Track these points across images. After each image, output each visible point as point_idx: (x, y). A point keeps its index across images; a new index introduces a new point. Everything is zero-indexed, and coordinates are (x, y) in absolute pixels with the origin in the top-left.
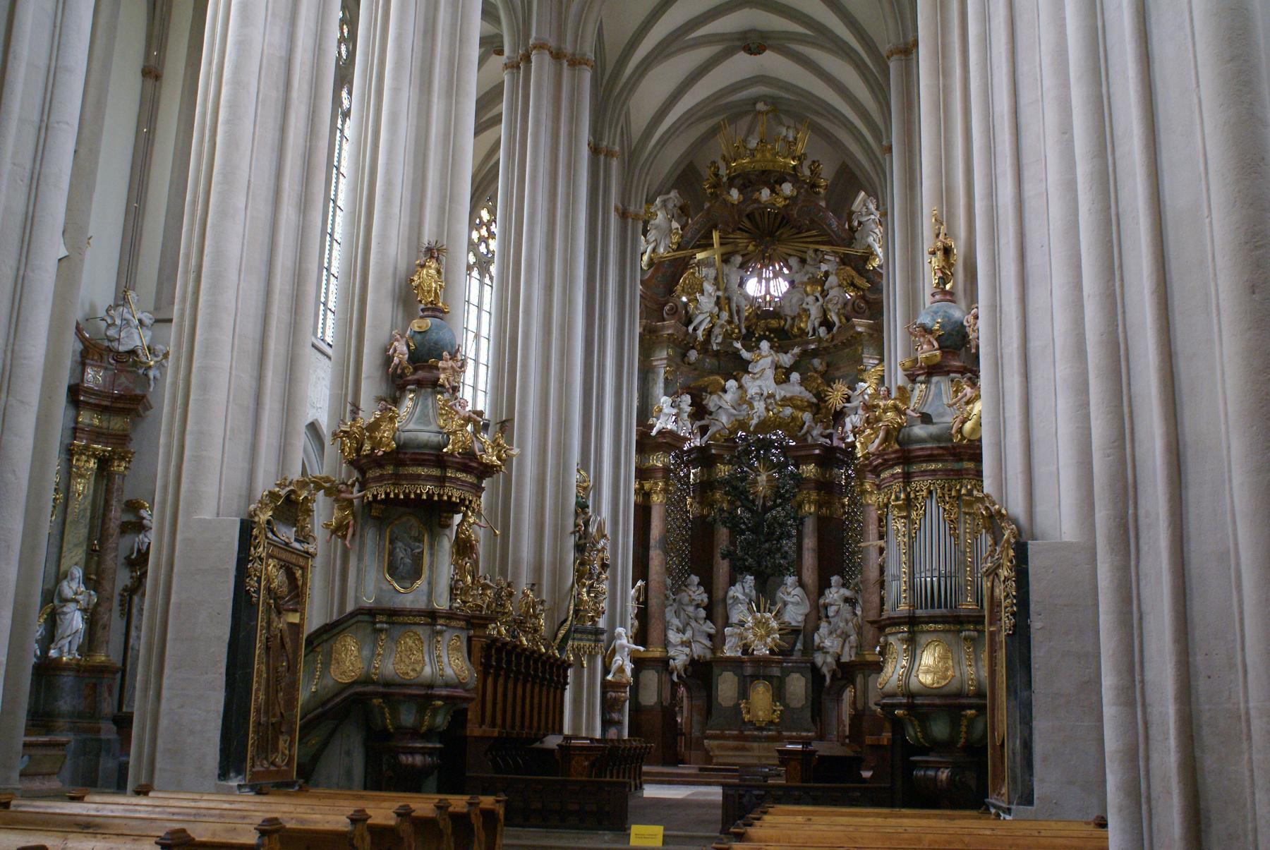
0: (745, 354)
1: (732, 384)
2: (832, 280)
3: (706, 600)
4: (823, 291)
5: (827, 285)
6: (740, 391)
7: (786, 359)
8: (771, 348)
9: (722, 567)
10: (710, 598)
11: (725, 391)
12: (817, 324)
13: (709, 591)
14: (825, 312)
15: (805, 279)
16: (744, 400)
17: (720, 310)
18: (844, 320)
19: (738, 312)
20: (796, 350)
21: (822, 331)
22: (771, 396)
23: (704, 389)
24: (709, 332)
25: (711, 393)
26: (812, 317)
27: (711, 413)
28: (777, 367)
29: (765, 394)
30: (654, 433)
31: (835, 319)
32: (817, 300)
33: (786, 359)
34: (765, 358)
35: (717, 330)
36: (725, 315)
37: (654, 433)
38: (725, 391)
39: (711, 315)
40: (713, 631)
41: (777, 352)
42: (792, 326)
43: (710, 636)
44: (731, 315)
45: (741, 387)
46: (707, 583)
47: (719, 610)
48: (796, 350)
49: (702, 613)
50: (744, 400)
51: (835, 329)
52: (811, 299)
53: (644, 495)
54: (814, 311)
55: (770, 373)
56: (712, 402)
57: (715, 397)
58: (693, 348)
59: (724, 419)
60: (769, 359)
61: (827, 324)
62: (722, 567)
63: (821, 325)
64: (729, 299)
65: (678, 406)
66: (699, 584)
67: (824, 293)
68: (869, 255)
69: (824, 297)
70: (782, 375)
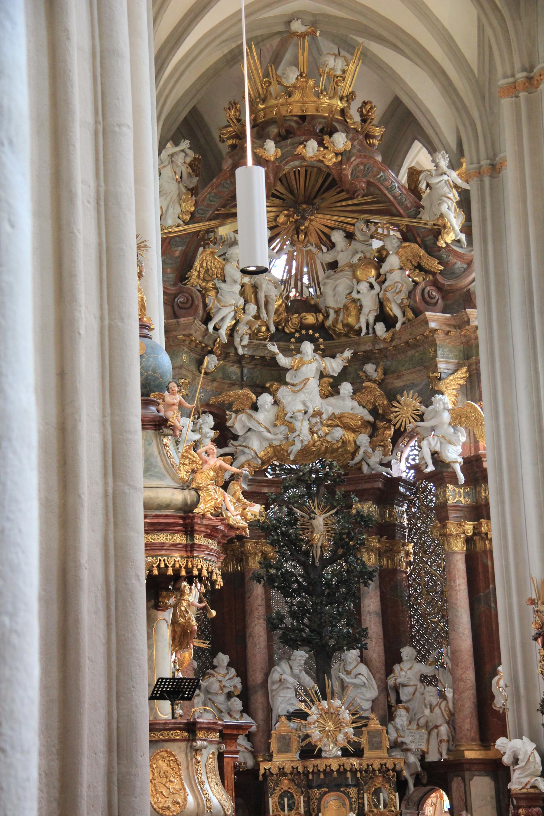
1: (266, 399)
4: (379, 275)
6: (276, 408)
7: (335, 366)
11: (255, 407)
21: (380, 328)
31: (396, 311)
32: (372, 287)
33: (335, 366)
35: (243, 329)
50: (283, 419)
51: (398, 325)
52: (363, 287)
55: (313, 384)
56: (238, 423)
57: (242, 417)
58: (211, 352)
60: (314, 365)
63: (377, 319)
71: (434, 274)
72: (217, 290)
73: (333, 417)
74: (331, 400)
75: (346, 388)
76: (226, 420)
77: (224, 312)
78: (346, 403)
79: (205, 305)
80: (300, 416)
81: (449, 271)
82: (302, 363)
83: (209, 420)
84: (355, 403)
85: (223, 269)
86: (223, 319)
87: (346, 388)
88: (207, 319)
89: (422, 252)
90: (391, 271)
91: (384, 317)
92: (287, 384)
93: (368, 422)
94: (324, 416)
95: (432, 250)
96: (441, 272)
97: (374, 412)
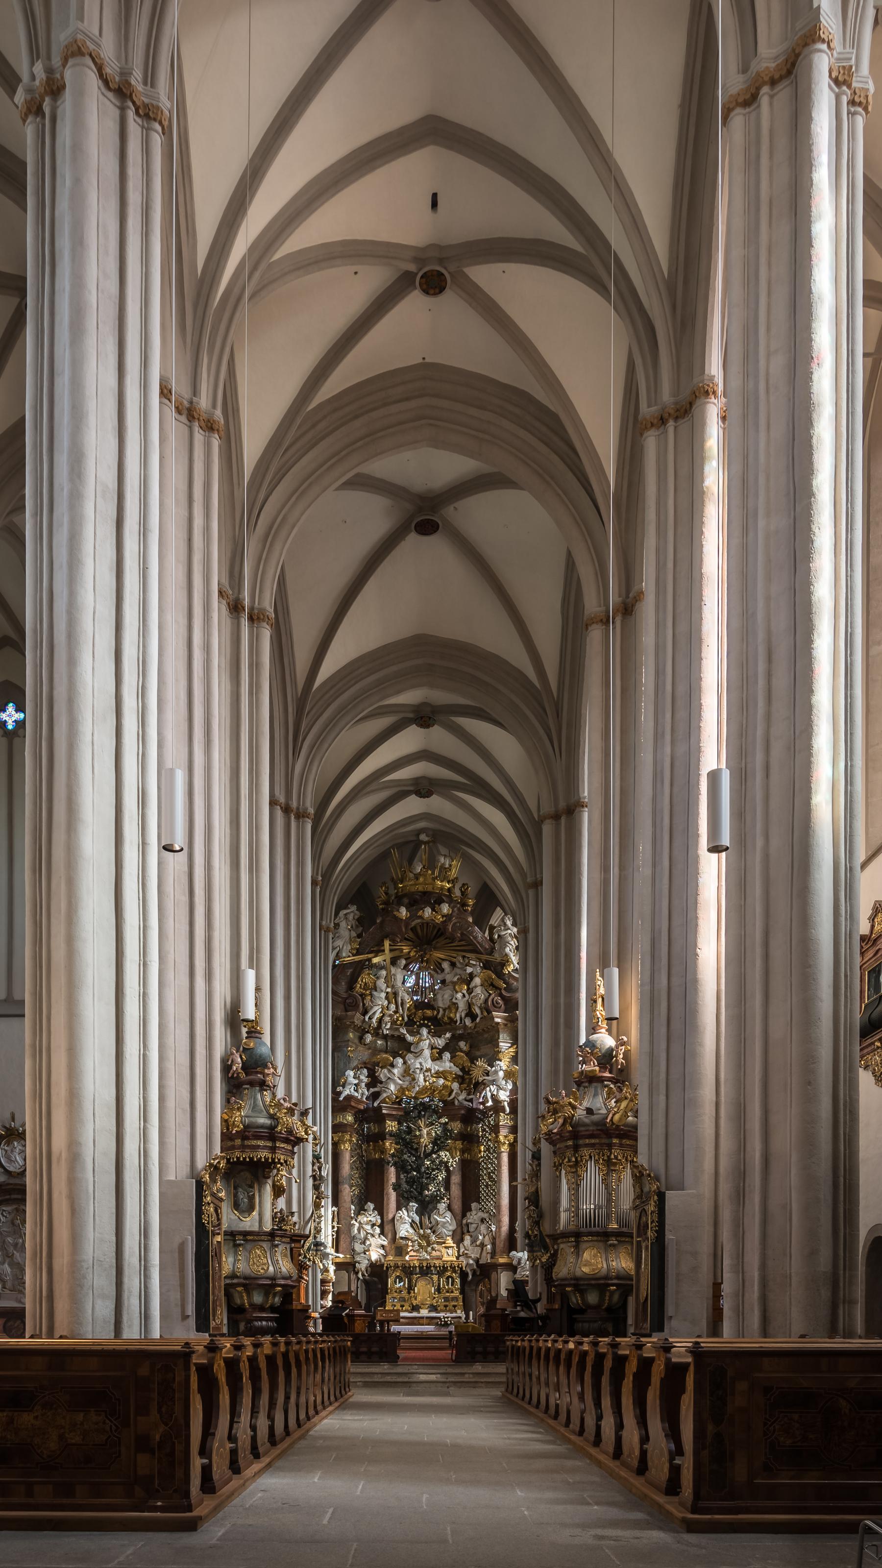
0: (409, 1038)
2: (477, 981)
3: (379, 1221)
4: (468, 989)
5: (472, 985)
7: (440, 1042)
8: (429, 1033)
9: (392, 1196)
10: (382, 1219)
11: (392, 1065)
12: (463, 1016)
13: (381, 1214)
14: (470, 1005)
15: (455, 979)
16: (407, 1072)
17: (389, 1003)
19: (402, 1004)
20: (448, 1035)
21: (468, 1022)
22: (429, 1070)
23: (378, 1064)
24: (380, 1021)
25: (382, 1068)
26: (460, 1010)
27: (381, 1082)
28: (432, 1047)
30: (341, 1099)
31: (478, 1011)
32: (464, 996)
33: (440, 1042)
34: (426, 1041)
35: (387, 1019)
36: (393, 1007)
37: (341, 1099)
38: (392, 1065)
39: (383, 1008)
42: (444, 1015)
44: (397, 1007)
45: (405, 1063)
46: (380, 1209)
48: (448, 1035)
49: (378, 1230)
50: (407, 1072)
51: (478, 1020)
52: (459, 995)
54: (462, 1005)
55: (427, 1053)
56: (383, 1074)
57: (385, 1071)
58: (368, 1032)
59: (392, 1087)
61: (471, 1015)
62: (392, 1196)
63: (467, 1015)
64: (395, 994)
65: (358, 1078)
67: (470, 991)
68: (505, 961)
69: (470, 994)
71: (500, 989)
72: (371, 995)
73: (437, 1073)
74: (438, 1062)
75: (447, 1055)
76: (375, 1072)
77: (376, 1008)
78: (446, 1064)
79: (364, 1005)
81: (509, 989)
82: (420, 1040)
83: (365, 1071)
84: (452, 1064)
85: (375, 983)
86: (375, 1013)
87: (447, 1055)
88: (365, 1012)
90: (476, 987)
91: (471, 1015)
92: (412, 1052)
93: (459, 1076)
94: (433, 1071)
96: (505, 989)
97: (462, 1069)
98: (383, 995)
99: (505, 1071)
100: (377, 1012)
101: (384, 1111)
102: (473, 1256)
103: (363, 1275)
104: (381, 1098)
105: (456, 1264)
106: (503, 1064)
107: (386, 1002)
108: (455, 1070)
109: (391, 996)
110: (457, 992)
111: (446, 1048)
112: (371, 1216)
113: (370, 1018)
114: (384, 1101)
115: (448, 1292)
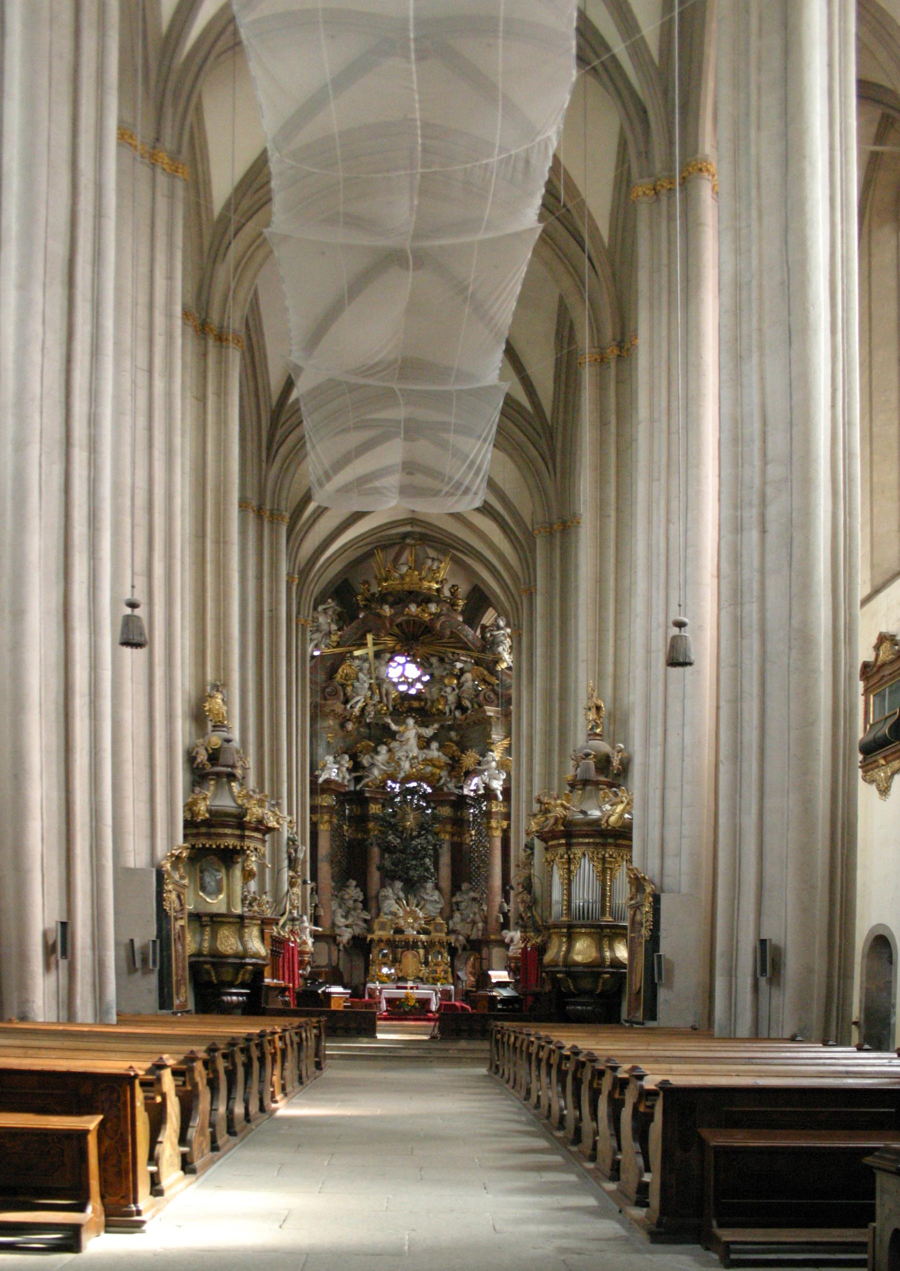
0: (394, 727)
4: (458, 683)
5: (463, 679)
8: (416, 723)
9: (375, 876)
10: (365, 895)
11: (377, 753)
15: (444, 674)
17: (373, 693)
18: (476, 706)
20: (436, 726)
24: (363, 710)
27: (364, 768)
28: (419, 737)
29: (411, 755)
31: (467, 703)
32: (454, 690)
33: (428, 732)
34: (411, 731)
39: (365, 698)
40: (368, 918)
41: (420, 726)
43: (365, 921)
44: (381, 697)
45: (390, 750)
46: (363, 885)
47: (373, 904)
49: (360, 905)
52: (449, 690)
53: (314, 825)
54: (452, 698)
55: (413, 742)
56: (365, 760)
57: (367, 756)
58: (349, 720)
60: (414, 731)
63: (457, 708)
66: (356, 886)
67: (460, 686)
70: (424, 743)
71: (493, 685)
74: (425, 751)
75: (434, 745)
77: (357, 698)
78: (434, 752)
80: (404, 758)
82: (407, 729)
84: (441, 754)
87: (434, 745)
89: (486, 673)
90: (466, 681)
95: (493, 672)
98: (367, 685)
99: (497, 762)
100: (359, 701)
101: (367, 795)
102: (462, 932)
103: (344, 947)
104: (363, 782)
105: (445, 940)
106: (496, 755)
107: (369, 693)
108: (444, 759)
109: (375, 687)
110: (446, 686)
111: (434, 737)
112: (353, 891)
113: (351, 707)
114: (367, 785)
115: (435, 965)
